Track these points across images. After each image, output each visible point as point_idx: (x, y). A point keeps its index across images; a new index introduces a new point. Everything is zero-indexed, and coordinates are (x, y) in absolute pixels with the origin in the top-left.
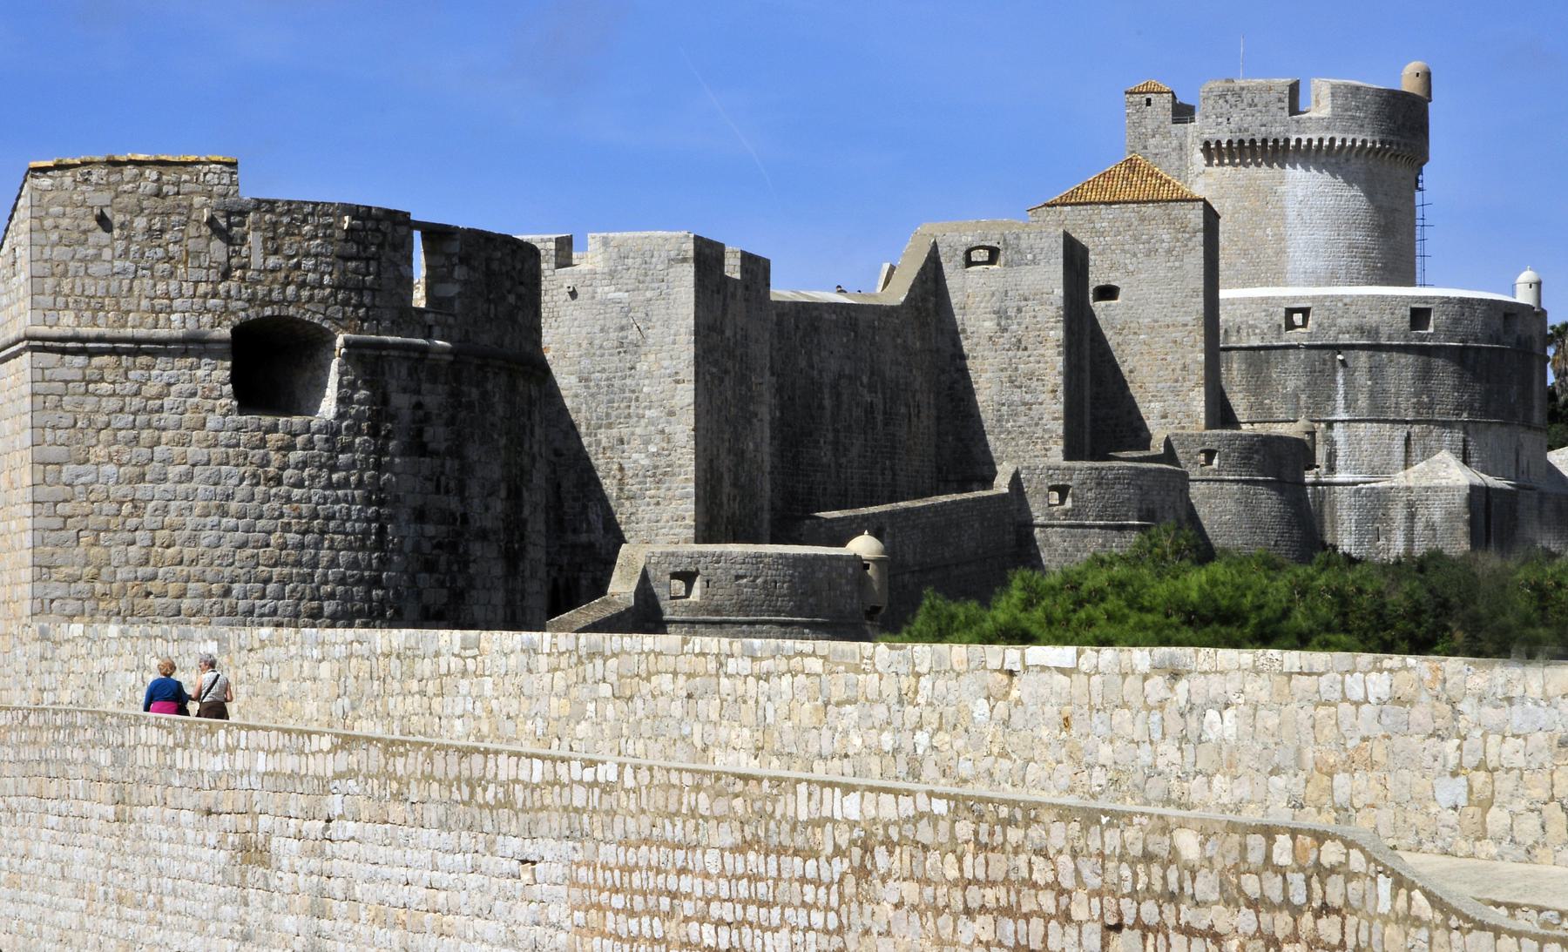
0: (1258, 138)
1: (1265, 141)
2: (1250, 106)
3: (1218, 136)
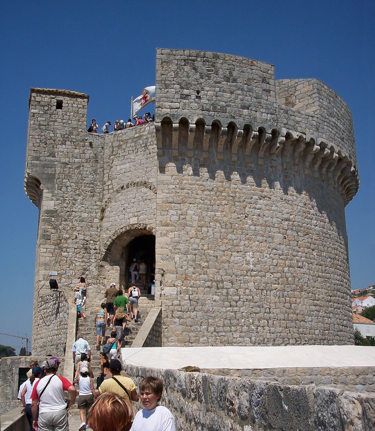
0: (240, 123)
1: (248, 128)
2: (227, 79)
3: (185, 113)
